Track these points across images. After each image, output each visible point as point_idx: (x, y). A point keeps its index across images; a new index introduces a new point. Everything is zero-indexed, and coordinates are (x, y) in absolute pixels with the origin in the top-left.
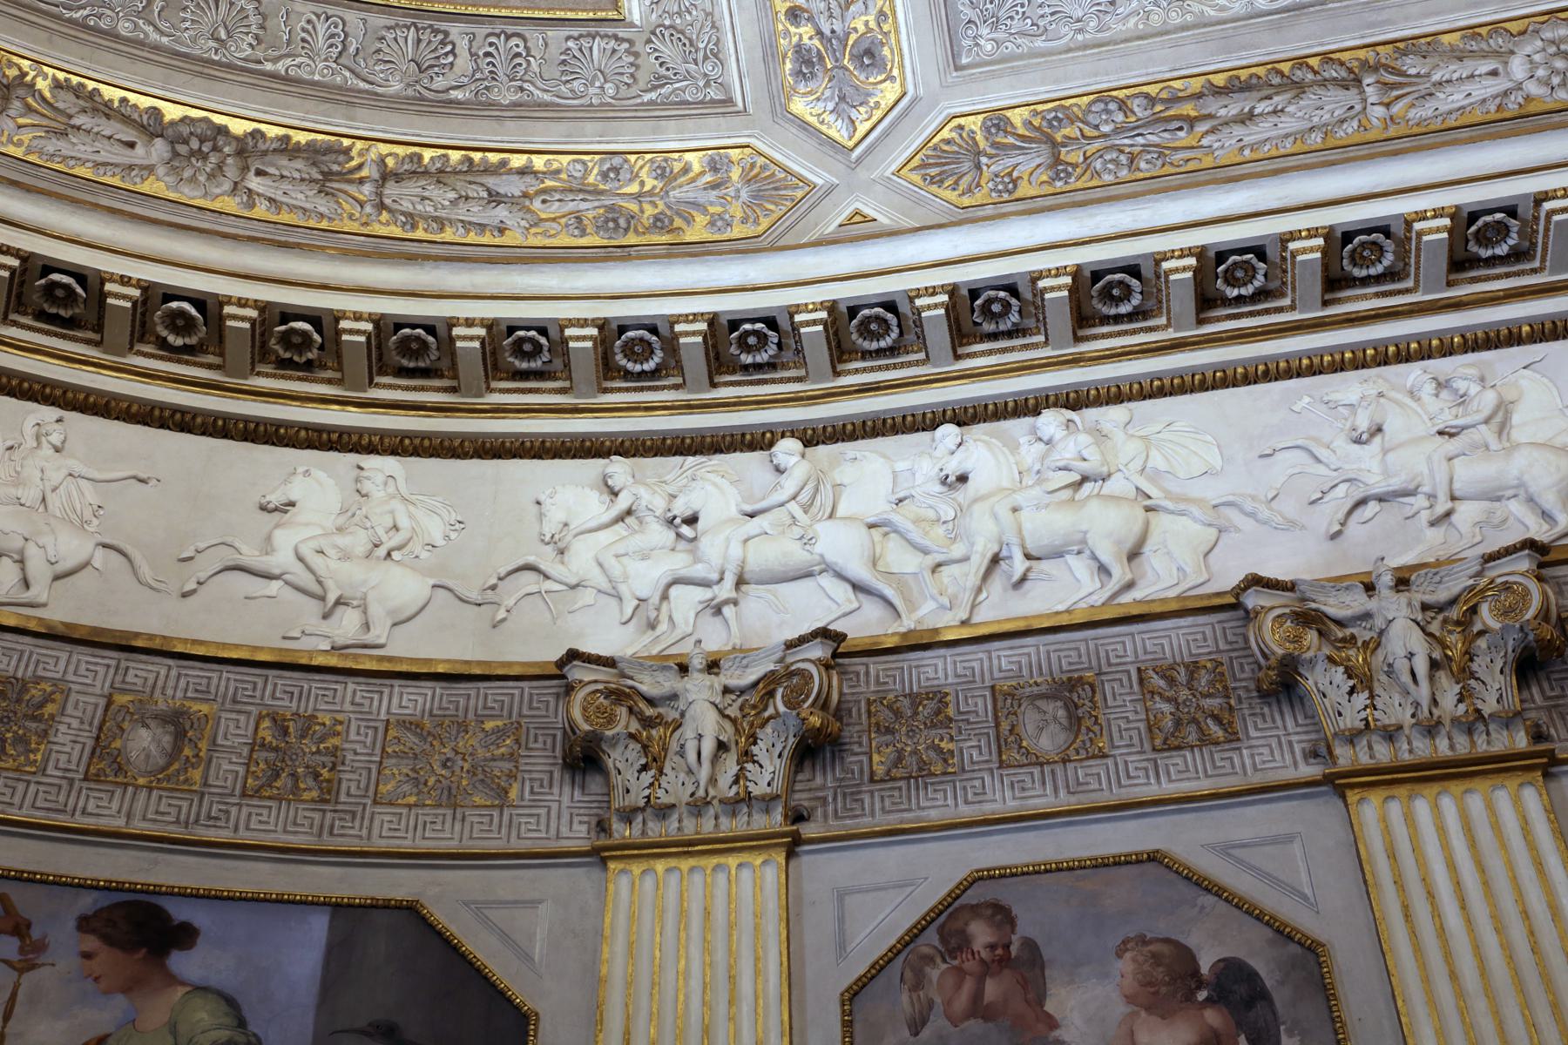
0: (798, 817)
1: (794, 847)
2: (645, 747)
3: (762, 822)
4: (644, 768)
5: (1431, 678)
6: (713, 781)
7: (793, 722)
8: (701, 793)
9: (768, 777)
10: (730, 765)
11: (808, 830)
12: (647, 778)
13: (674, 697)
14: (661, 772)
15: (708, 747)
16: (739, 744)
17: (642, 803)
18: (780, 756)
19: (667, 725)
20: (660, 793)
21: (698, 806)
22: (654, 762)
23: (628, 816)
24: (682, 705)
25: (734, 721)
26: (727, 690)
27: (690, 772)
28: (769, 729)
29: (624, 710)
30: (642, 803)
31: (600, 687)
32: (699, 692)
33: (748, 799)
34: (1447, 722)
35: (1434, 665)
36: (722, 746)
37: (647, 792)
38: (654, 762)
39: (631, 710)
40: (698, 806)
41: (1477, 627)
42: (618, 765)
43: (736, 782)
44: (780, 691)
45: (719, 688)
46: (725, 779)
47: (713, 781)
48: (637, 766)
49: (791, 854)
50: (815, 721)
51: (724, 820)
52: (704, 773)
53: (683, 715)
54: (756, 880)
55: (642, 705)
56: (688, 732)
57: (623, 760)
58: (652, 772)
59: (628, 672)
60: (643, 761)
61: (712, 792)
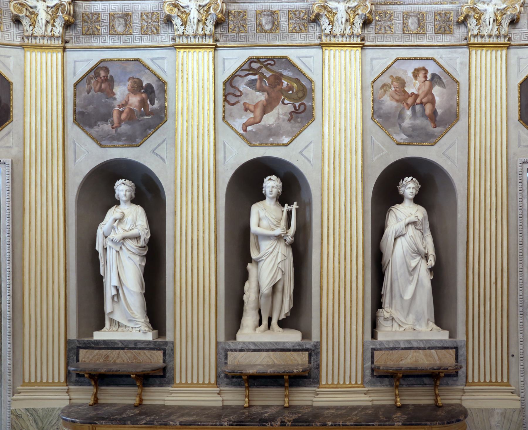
1: (216, 48)
2: (182, 19)
4: (182, 25)
5: (345, 23)
7: (215, 16)
8: (195, 32)
10: (201, 26)
12: (183, 27)
13: (188, 6)
17: (182, 34)
19: (187, 14)
20: (186, 31)
24: (190, 8)
25: (202, 14)
28: (209, 17)
33: (205, 35)
34: (346, 35)
35: (347, 21)
41: (357, 13)
44: (212, 8)
45: (198, 5)
47: (197, 30)
49: (215, 50)
50: (220, 16)
52: (195, 27)
54: (207, 55)
55: (181, 8)
56: (191, 16)
57: (177, 22)
58: (184, 26)
61: (197, 32)
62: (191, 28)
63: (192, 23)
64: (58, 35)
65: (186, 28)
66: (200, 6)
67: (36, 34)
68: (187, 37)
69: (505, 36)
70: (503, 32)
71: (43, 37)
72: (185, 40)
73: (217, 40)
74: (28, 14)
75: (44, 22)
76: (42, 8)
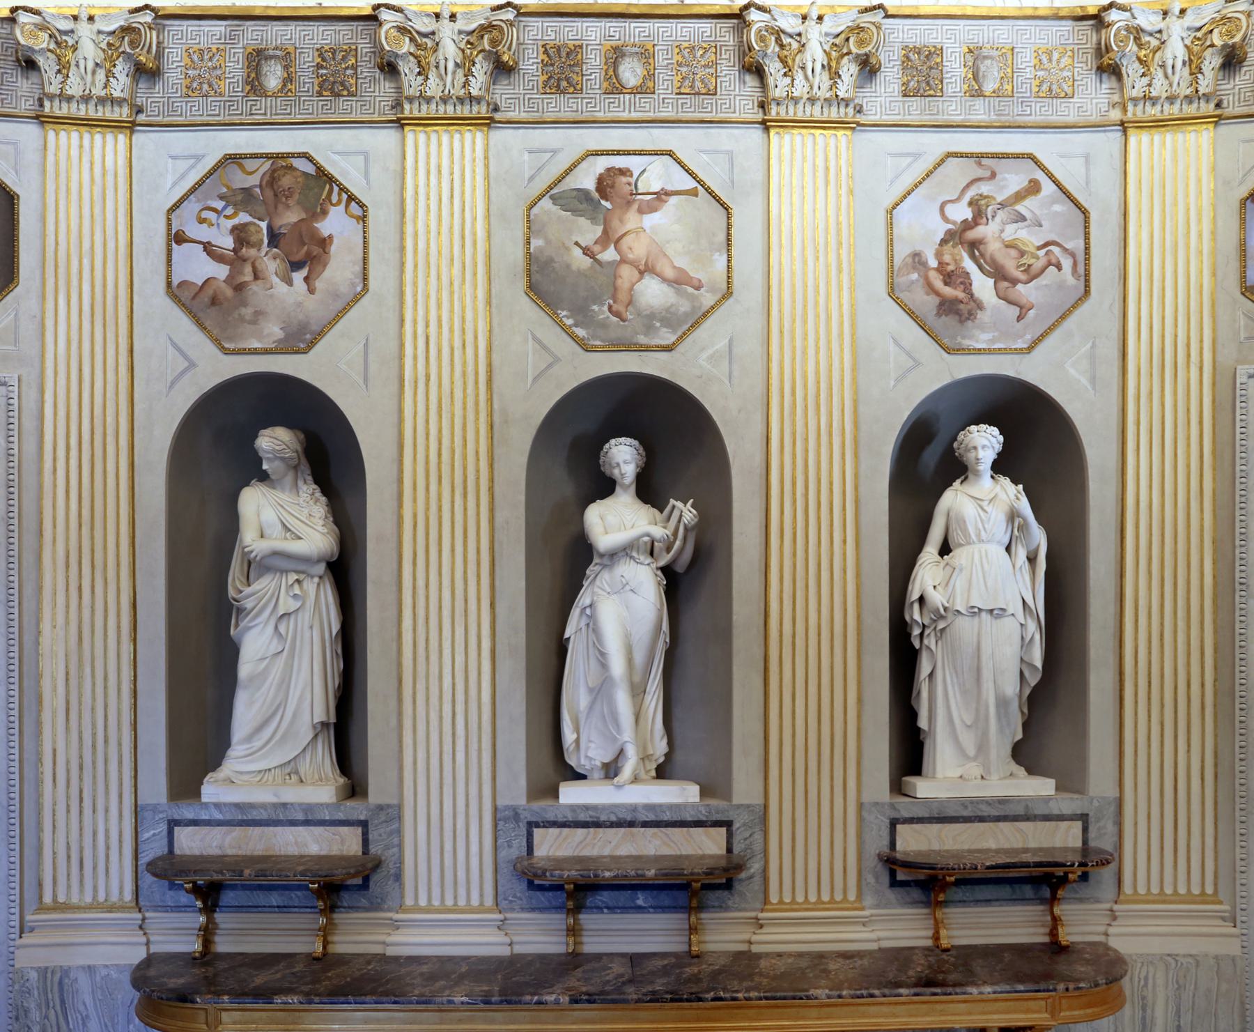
0: (140, 111)
4: (419, 73)
9: (479, 85)
11: (142, 118)
13: (433, 33)
14: (427, 78)
15: (451, 65)
16: (466, 65)
21: (444, 100)
22: (423, 72)
23: (410, 100)
25: (463, 51)
26: (99, 32)
28: (480, 56)
29: (407, 40)
32: (447, 32)
36: (457, 65)
38: (423, 72)
39: (411, 40)
40: (444, 100)
43: (105, 87)
46: (100, 85)
51: (459, 108)
53: (437, 44)
63: (443, 72)
64: (122, 95)
66: (460, 32)
67: (69, 92)
68: (429, 100)
69: (1207, 97)
70: (1202, 90)
71: (86, 99)
72: (424, 107)
74: (53, 46)
75: (90, 65)
76: (88, 33)
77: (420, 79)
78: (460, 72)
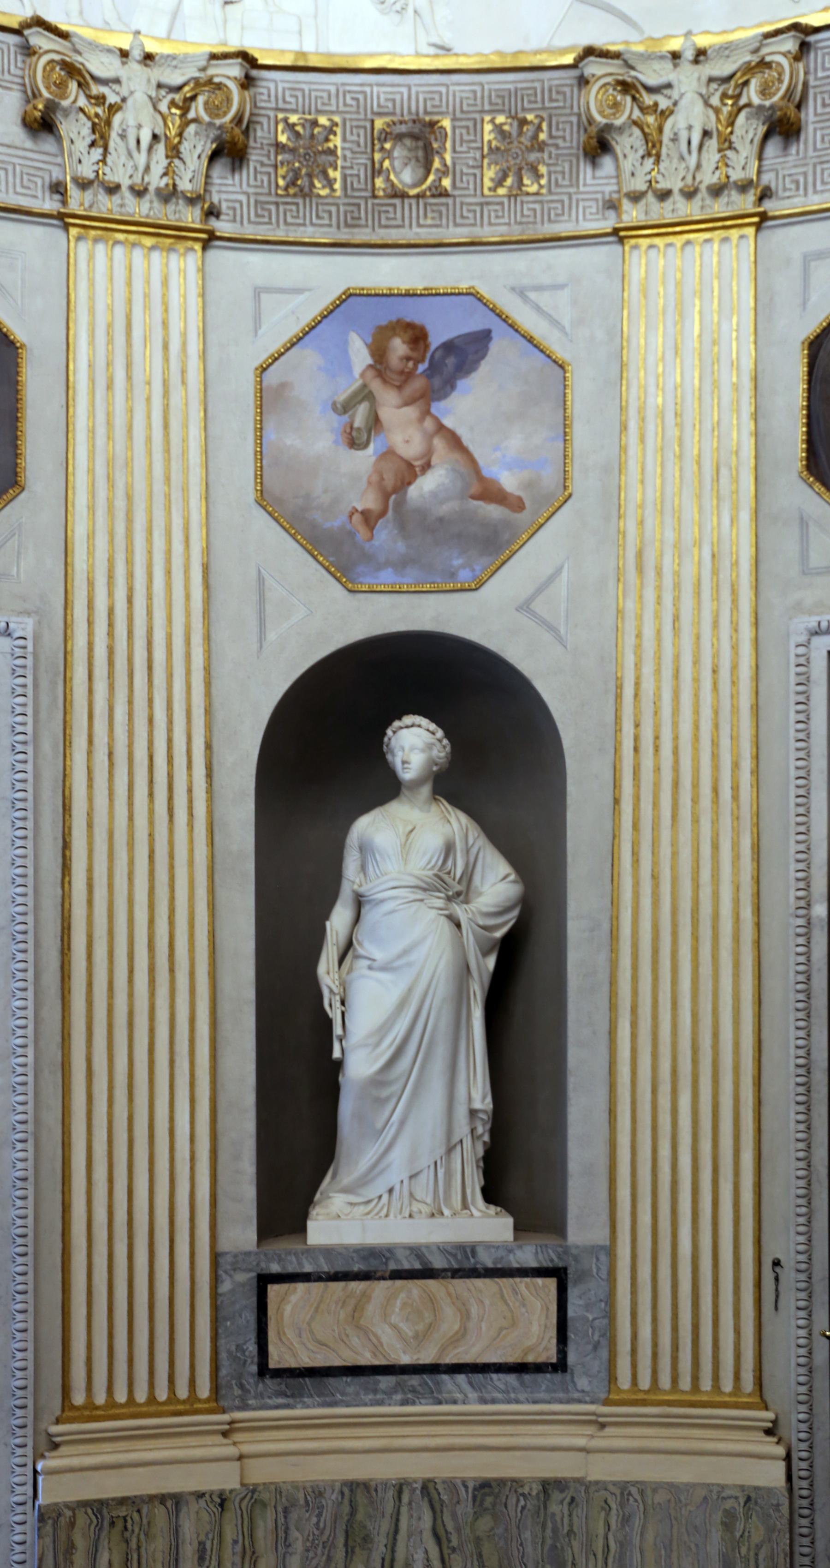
3: (191, 217)
6: (147, 169)
15: (146, 138)
18: (199, 157)
20: (107, 170)
27: (130, 155)
30: (92, 176)
31: (57, 57)
37: (95, 167)
42: (72, 136)
47: (147, 169)
48: (88, 141)
52: (141, 159)
57: (75, 130)
59: (78, 47)
60: (93, 137)
62: (123, 159)
65: (109, 160)
73: (212, 212)
77: (97, 153)
78: (161, 148)
